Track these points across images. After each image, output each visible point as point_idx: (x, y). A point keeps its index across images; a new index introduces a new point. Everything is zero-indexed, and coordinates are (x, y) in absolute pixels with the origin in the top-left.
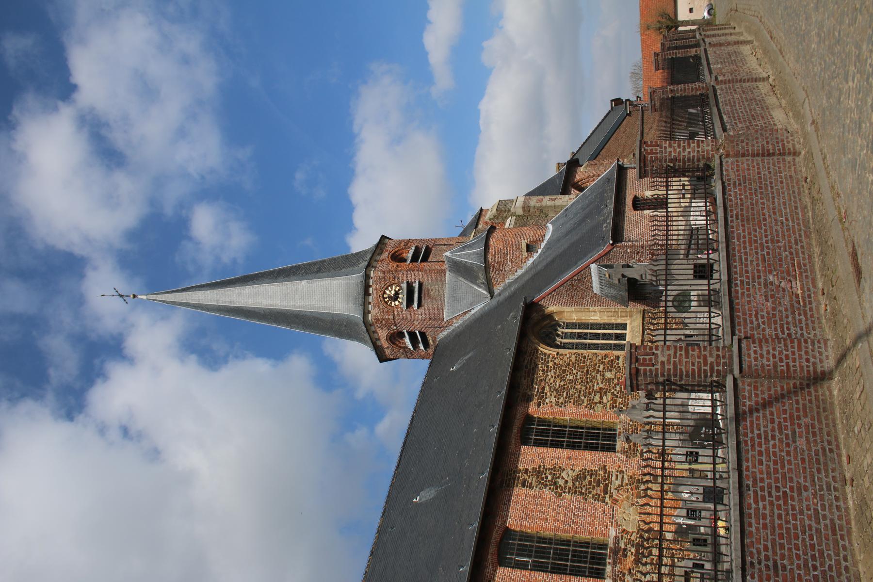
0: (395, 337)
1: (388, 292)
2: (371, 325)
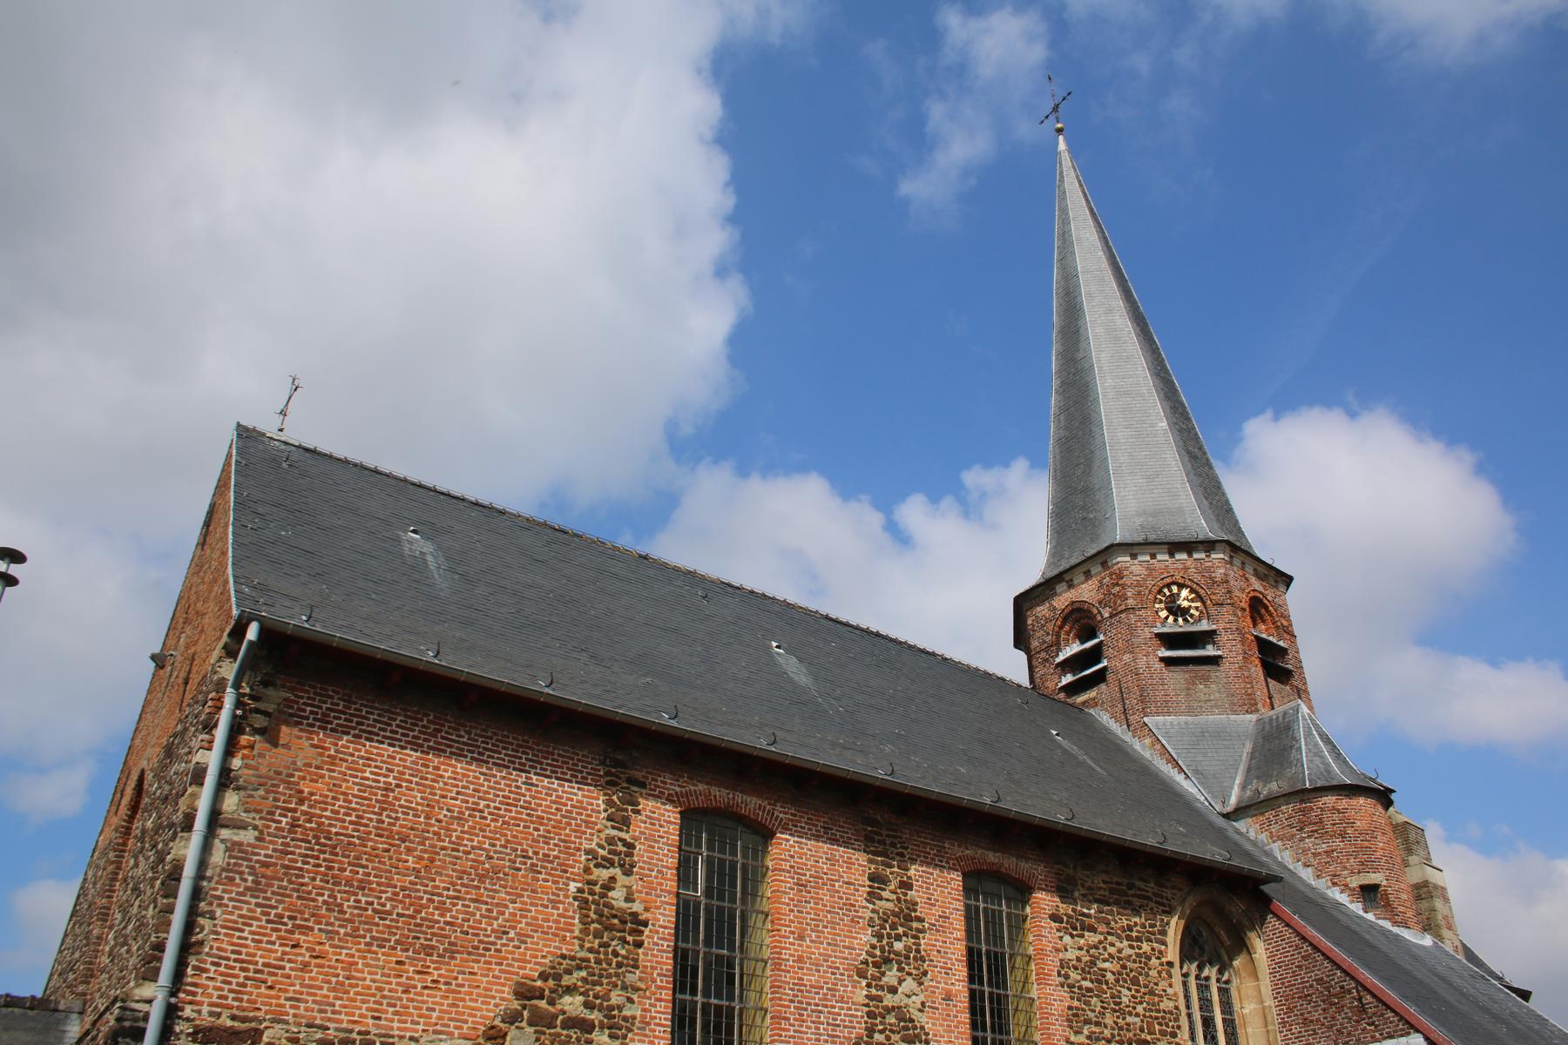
0: (1082, 621)
1: (1185, 593)
2: (1104, 564)
